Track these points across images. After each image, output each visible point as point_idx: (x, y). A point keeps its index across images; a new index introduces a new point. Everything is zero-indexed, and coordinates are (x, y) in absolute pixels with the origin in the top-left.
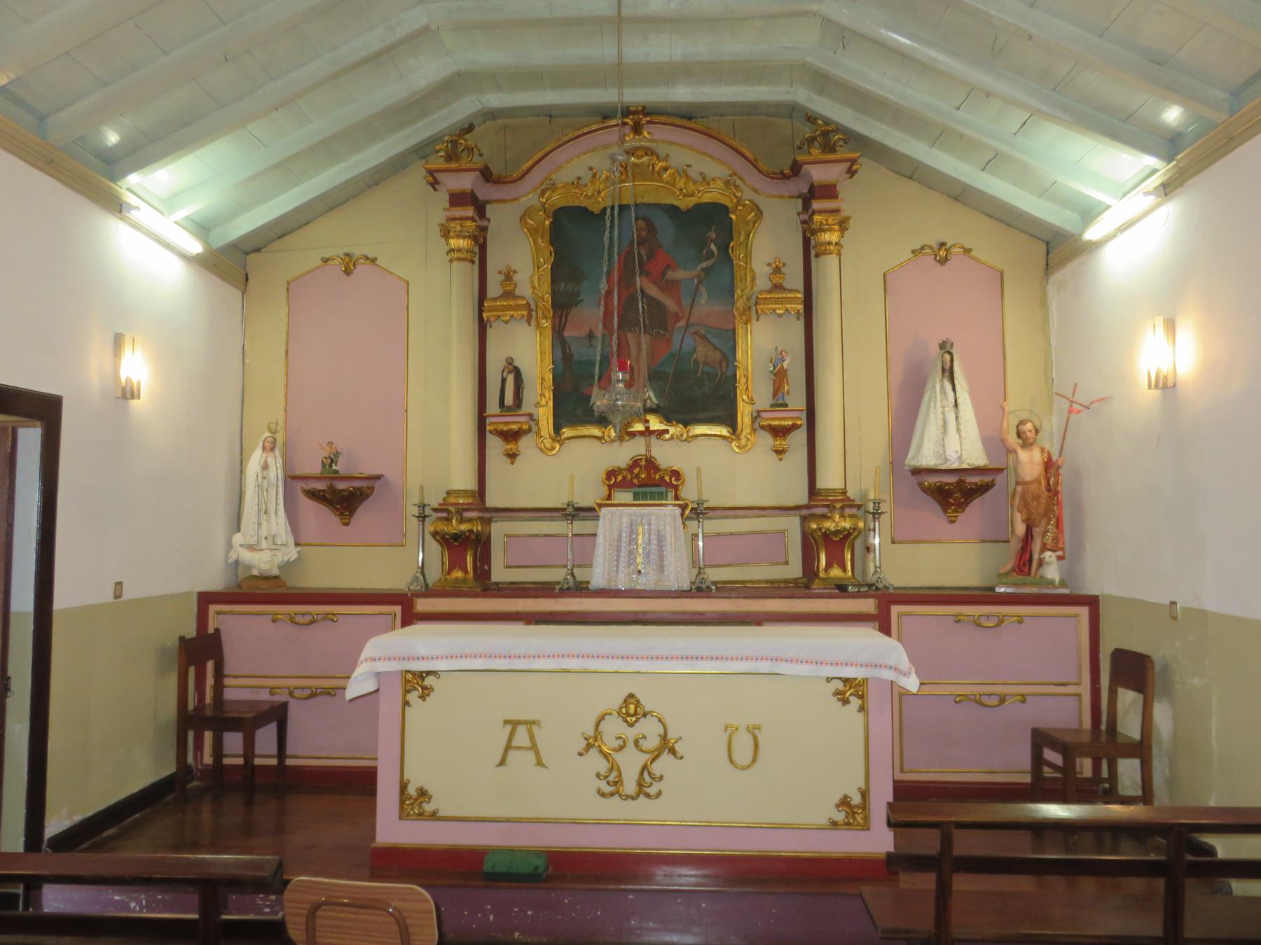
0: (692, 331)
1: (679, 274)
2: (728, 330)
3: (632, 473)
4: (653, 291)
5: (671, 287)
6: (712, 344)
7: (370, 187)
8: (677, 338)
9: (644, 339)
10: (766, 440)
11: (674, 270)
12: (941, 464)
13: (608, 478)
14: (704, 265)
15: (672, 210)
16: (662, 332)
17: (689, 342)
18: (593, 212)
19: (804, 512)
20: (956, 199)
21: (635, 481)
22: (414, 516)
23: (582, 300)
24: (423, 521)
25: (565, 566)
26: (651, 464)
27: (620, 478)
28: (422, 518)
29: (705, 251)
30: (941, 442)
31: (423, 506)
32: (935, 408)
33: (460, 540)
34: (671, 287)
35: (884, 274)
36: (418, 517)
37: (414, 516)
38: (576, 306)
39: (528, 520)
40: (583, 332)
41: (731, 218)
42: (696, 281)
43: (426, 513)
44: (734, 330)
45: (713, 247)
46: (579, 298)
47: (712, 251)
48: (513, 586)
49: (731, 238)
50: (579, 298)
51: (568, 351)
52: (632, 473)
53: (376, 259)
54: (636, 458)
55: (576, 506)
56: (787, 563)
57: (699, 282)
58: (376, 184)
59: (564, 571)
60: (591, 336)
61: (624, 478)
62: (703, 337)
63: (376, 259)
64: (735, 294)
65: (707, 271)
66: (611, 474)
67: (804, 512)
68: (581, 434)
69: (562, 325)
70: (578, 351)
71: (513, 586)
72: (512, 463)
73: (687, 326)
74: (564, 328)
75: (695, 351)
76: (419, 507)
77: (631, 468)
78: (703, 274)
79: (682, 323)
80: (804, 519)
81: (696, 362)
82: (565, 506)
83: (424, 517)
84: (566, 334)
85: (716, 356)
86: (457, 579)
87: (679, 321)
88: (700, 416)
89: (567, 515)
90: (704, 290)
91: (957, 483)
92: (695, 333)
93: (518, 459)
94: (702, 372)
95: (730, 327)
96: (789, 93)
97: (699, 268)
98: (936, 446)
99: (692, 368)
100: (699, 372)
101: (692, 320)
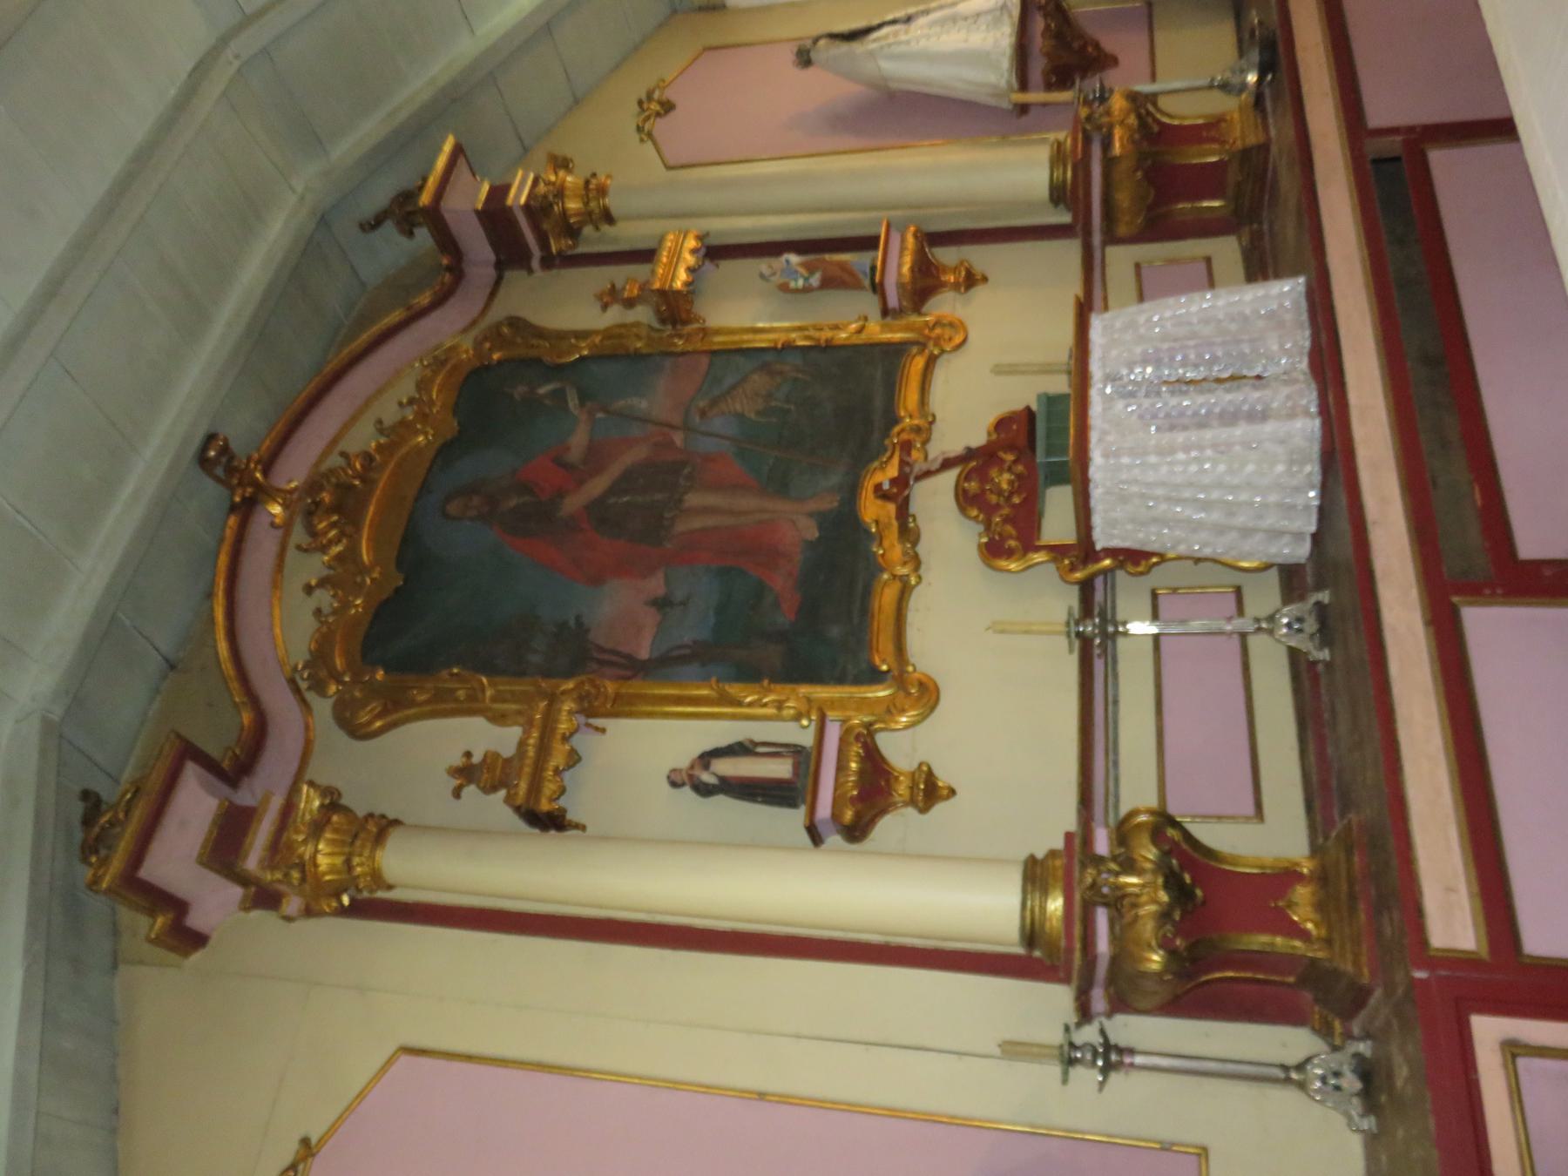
0: (697, 419)
1: (578, 440)
2: (711, 365)
3: (998, 507)
4: (597, 486)
5: (596, 458)
6: (734, 387)
7: (114, 1131)
8: (707, 445)
9: (693, 499)
10: (944, 305)
11: (568, 449)
12: (1011, 16)
13: (1009, 554)
14: (573, 402)
15: (446, 453)
16: (686, 471)
17: (717, 424)
18: (397, 590)
19: (1097, 239)
20: (577, 102)
21: (1016, 500)
22: (1102, 1084)
23: (578, 618)
24: (1121, 1051)
25: (1243, 636)
26: (977, 462)
27: (1009, 529)
28: (1112, 1058)
29: (547, 402)
30: (969, 21)
31: (1068, 1059)
32: (908, 42)
33: (1187, 878)
34: (596, 458)
35: (669, 168)
36: (1107, 1070)
37: (1102, 1084)
38: (588, 631)
39: (1116, 764)
40: (650, 619)
41: (500, 362)
42: (600, 415)
43: (1097, 1040)
44: (714, 353)
45: (542, 391)
46: (572, 623)
47: (554, 393)
48: (1317, 804)
49: (538, 361)
50: (572, 623)
51: (687, 651)
52: (998, 507)
53: (305, 1142)
54: (961, 498)
55: (1076, 614)
56: (1208, 260)
57: (607, 412)
58: (116, 1111)
59: (1257, 644)
60: (662, 604)
61: (1006, 520)
62: (714, 402)
63: (305, 1142)
64: (645, 351)
65: (584, 397)
66: (993, 551)
67: (1097, 239)
68: (891, 621)
69: (622, 661)
70: (692, 628)
71: (1317, 804)
72: (952, 792)
73: (687, 428)
74: (629, 657)
75: (741, 417)
76: (1071, 1062)
77: (988, 510)
78: (589, 404)
79: (678, 438)
80: (1111, 238)
81: (758, 413)
82: (1077, 644)
83: (1108, 1047)
84: (644, 654)
85: (759, 381)
86: (1320, 906)
87: (673, 442)
88: (878, 403)
89: (1105, 636)
90: (621, 403)
91: (1046, 19)
92: (703, 414)
93: (944, 778)
94: (788, 401)
95: (705, 360)
96: (302, 198)
97: (576, 412)
98: (978, 29)
99: (774, 420)
100: (786, 406)
101: (676, 419)
